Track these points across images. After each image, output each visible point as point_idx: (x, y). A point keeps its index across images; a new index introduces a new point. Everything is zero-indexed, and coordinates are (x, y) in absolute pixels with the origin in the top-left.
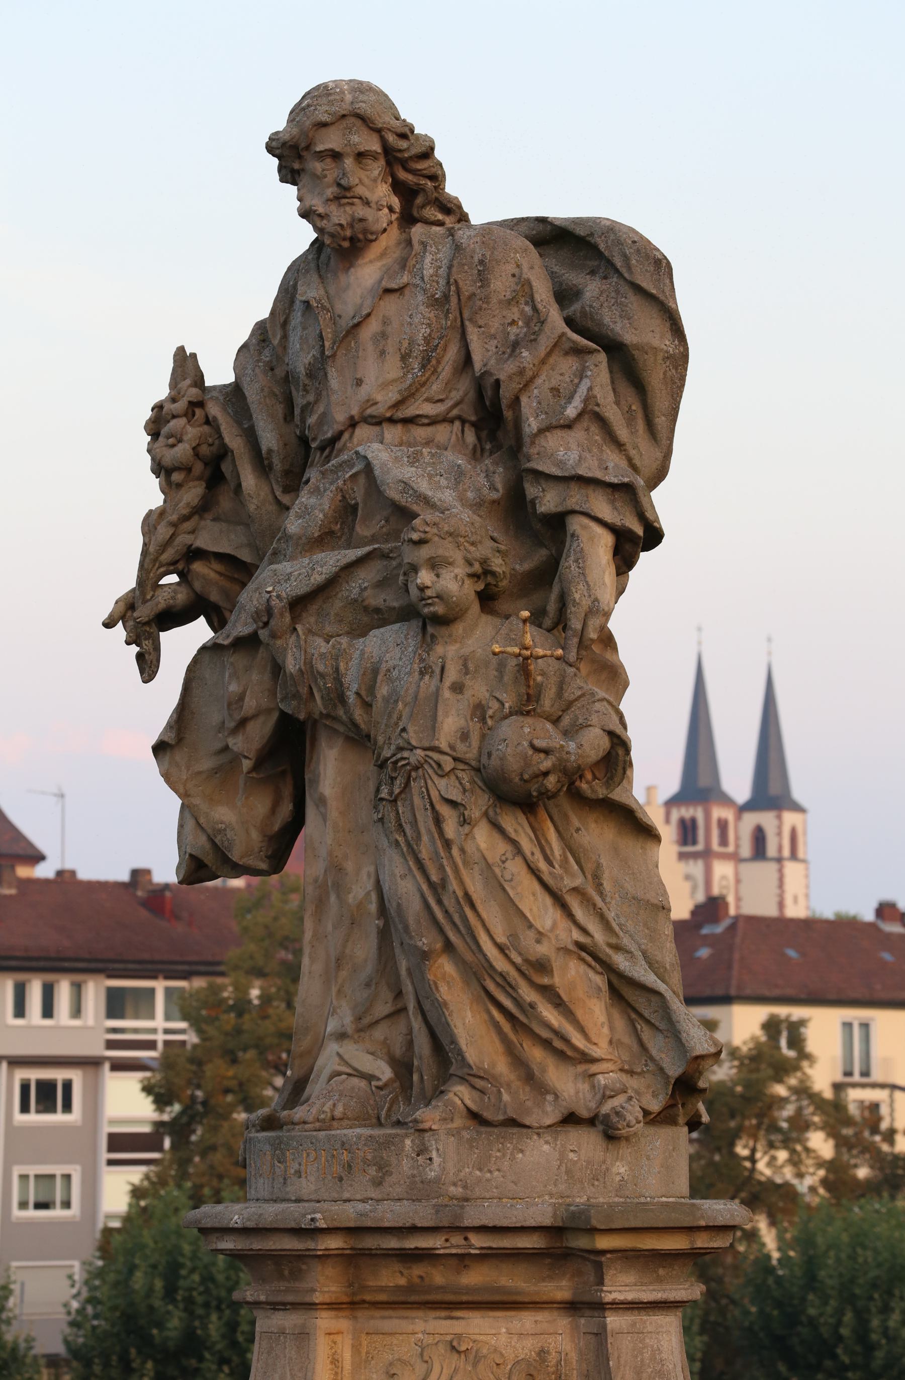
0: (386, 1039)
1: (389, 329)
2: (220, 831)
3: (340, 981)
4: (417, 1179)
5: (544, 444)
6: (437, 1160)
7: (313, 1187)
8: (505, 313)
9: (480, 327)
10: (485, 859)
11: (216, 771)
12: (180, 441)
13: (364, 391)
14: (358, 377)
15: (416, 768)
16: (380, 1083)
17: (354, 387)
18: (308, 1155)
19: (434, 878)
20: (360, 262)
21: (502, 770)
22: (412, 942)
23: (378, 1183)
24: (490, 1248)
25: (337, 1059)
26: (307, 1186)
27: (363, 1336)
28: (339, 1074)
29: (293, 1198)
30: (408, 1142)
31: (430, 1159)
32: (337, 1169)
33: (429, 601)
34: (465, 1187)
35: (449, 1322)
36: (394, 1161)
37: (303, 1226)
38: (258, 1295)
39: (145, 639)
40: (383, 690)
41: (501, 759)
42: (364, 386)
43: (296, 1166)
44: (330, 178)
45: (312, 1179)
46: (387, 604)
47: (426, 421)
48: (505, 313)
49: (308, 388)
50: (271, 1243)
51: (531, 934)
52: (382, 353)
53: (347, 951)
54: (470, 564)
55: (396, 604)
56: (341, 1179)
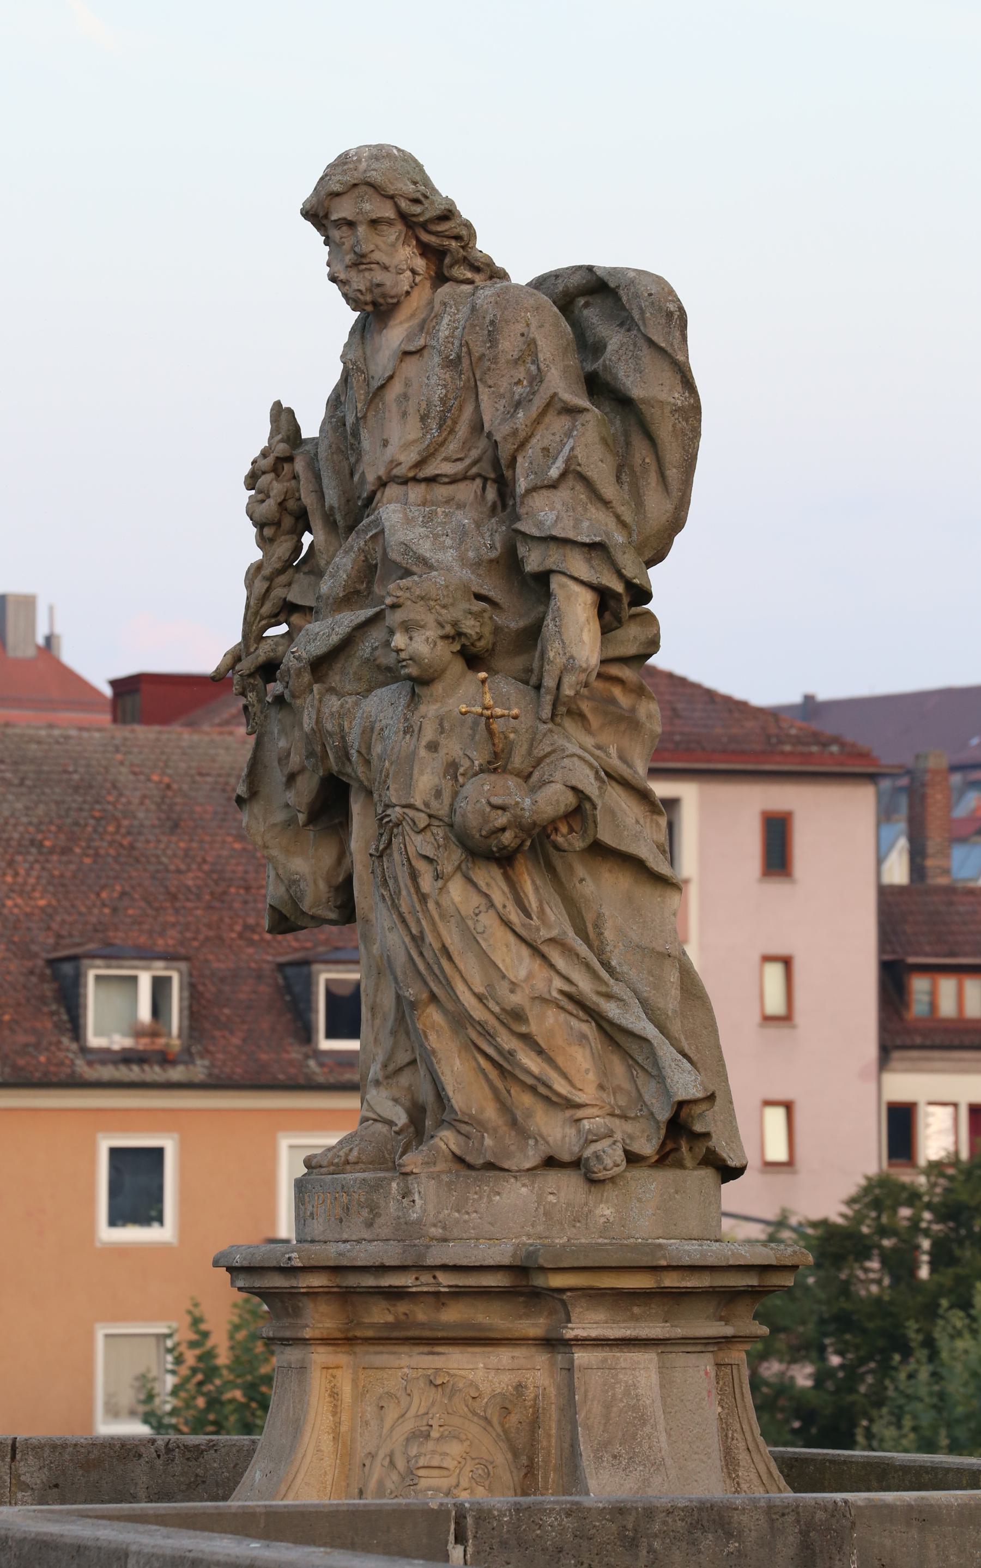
0: (411, 1085)
4: (402, 1220)
5: (531, 504)
8: (512, 373)
9: (490, 387)
10: (459, 912)
12: (268, 497)
13: (391, 450)
14: (385, 437)
15: (397, 825)
19: (414, 931)
20: (392, 323)
21: (464, 826)
23: (369, 1225)
24: (457, 1286)
30: (394, 1185)
31: (414, 1201)
32: (339, 1211)
33: (404, 663)
34: (444, 1228)
35: (430, 1357)
36: (382, 1204)
39: (250, 692)
40: (377, 749)
42: (389, 447)
44: (347, 246)
45: (321, 1220)
47: (446, 480)
48: (512, 373)
50: (266, 1282)
51: (505, 984)
52: (404, 414)
53: (378, 1000)
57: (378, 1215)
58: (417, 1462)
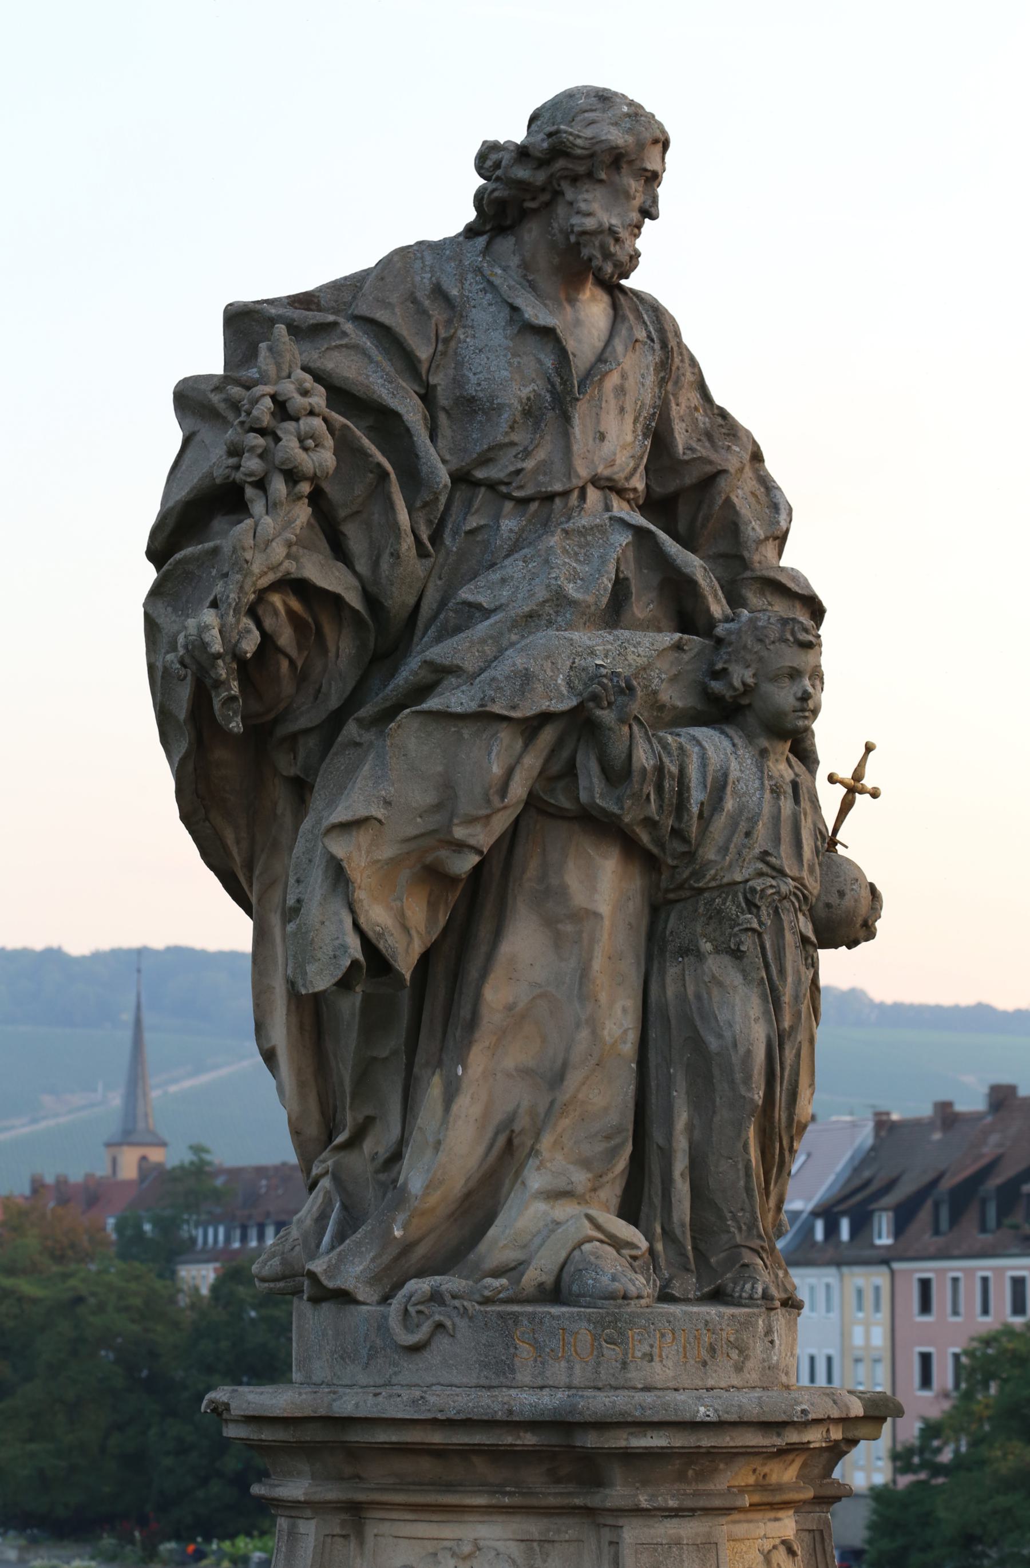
1: (627, 385)
3: (559, 1129)
5: (764, 553)
7: (670, 1373)
13: (607, 447)
16: (634, 1252)
17: (597, 441)
18: (663, 1335)
19: (786, 1024)
22: (750, 1095)
23: (739, 1369)
26: (662, 1372)
28: (590, 1240)
29: (640, 1386)
30: (760, 1322)
36: (752, 1344)
37: (796, 1419)
38: (666, 1501)
41: (856, 901)
42: (606, 442)
43: (646, 1348)
45: (670, 1364)
49: (516, 426)
50: (728, 1439)
55: (679, 704)
56: (705, 1364)
57: (747, 1358)
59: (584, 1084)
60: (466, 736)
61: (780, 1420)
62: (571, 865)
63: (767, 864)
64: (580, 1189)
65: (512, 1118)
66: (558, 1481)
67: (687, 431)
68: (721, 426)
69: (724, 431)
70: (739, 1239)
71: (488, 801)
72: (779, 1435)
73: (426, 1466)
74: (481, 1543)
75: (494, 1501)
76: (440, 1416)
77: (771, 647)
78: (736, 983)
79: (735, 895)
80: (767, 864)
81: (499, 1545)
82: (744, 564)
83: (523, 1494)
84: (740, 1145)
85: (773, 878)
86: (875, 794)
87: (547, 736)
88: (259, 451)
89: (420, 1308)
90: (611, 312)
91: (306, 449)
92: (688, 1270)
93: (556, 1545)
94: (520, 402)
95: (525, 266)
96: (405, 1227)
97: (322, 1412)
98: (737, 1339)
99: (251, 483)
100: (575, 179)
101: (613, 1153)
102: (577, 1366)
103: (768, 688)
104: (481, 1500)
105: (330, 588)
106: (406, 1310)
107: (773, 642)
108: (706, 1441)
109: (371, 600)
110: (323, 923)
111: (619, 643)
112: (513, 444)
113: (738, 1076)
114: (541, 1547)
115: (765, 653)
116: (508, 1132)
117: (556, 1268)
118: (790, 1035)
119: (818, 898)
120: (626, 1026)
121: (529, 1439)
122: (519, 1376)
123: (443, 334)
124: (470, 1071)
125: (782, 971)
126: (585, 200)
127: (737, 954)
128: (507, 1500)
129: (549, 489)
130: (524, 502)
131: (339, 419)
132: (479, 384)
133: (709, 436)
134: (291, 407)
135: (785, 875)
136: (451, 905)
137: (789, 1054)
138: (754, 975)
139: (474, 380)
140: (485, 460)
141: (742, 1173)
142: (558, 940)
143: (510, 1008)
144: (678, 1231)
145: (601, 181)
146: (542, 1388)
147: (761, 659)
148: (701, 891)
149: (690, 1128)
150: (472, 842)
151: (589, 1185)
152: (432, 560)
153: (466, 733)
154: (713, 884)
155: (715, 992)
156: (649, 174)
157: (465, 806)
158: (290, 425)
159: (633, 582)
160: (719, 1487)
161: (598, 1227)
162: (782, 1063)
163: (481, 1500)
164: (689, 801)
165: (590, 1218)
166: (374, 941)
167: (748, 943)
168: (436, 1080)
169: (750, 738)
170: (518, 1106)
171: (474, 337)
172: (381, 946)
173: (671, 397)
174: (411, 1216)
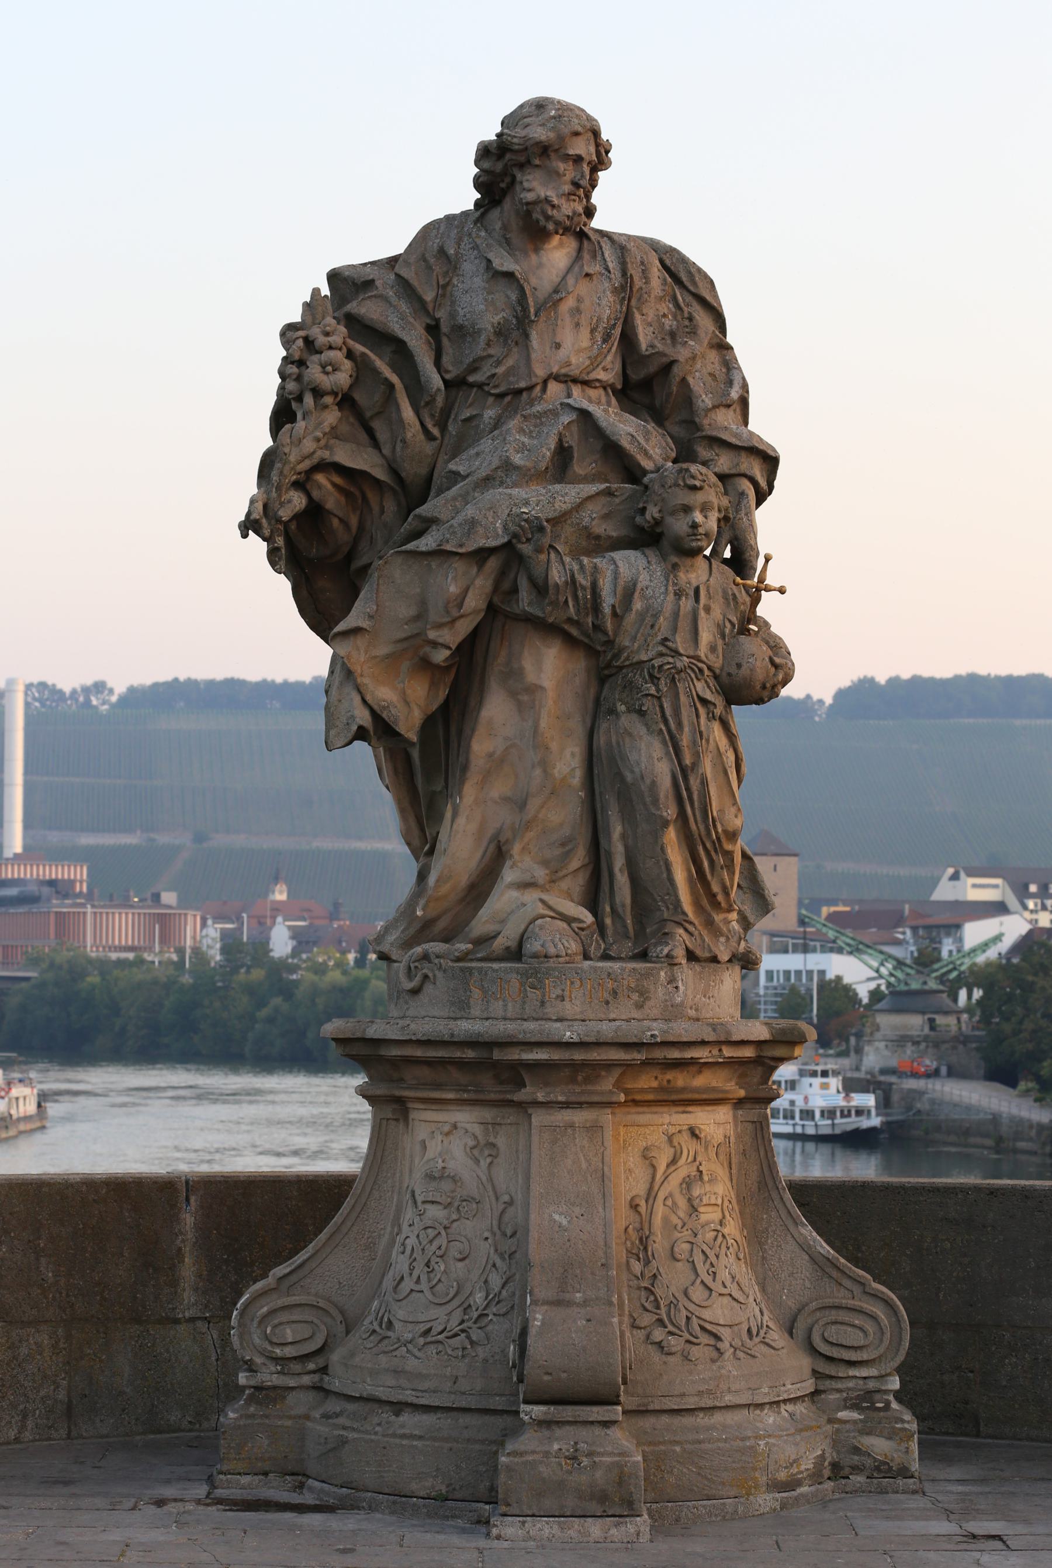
0: (569, 889)
1: (582, 306)
2: (384, 707)
3: (526, 840)
5: (714, 417)
6: (682, 988)
7: (578, 1009)
8: (657, 306)
10: (718, 749)
11: (388, 656)
13: (562, 353)
14: (557, 341)
15: (680, 672)
17: (553, 349)
18: (572, 983)
19: (688, 761)
20: (546, 246)
21: (751, 678)
22: (659, 813)
23: (639, 1006)
24: (732, 1057)
25: (540, 904)
26: (570, 1009)
27: (621, 1128)
28: (543, 917)
29: (554, 1018)
30: (662, 974)
31: (677, 988)
33: (699, 537)
34: (697, 1010)
35: (684, 1116)
36: (652, 987)
37: (645, 1041)
38: (557, 1096)
40: (638, 605)
41: (751, 670)
44: (569, 177)
45: (578, 1003)
46: (607, 533)
48: (658, 306)
49: (491, 343)
51: (733, 810)
53: (540, 816)
54: (719, 511)
55: (614, 534)
56: (607, 1003)
57: (648, 998)
58: (701, 1200)
59: (542, 807)
60: (434, 567)
61: (631, 1041)
62: (526, 653)
63: (667, 647)
64: (541, 881)
65: (499, 831)
66: (502, 1083)
67: (654, 333)
68: (687, 326)
69: (687, 330)
70: (666, 915)
71: (448, 612)
72: (639, 1052)
73: (425, 1072)
74: (459, 1125)
75: (458, 1096)
76: (414, 1038)
77: (669, 491)
78: (641, 734)
79: (643, 671)
80: (667, 647)
81: (468, 1126)
82: (698, 428)
83: (475, 1091)
84: (658, 849)
85: (673, 657)
86: (782, 591)
87: (493, 564)
88: (294, 377)
89: (416, 964)
90: (574, 254)
91: (327, 373)
92: (628, 938)
93: (503, 1127)
94: (493, 326)
95: (505, 228)
96: (423, 909)
97: (358, 1035)
98: (637, 986)
99: (293, 399)
100: (521, 166)
101: (567, 856)
102: (510, 1004)
103: (669, 520)
104: (451, 1096)
105: (357, 467)
106: (410, 968)
107: (670, 487)
108: (578, 1056)
109: (394, 472)
110: (340, 701)
111: (550, 494)
112: (490, 356)
113: (648, 800)
114: (493, 1128)
115: (665, 495)
116: (496, 842)
117: (517, 937)
118: (693, 770)
119: (722, 669)
120: (573, 766)
121: (470, 1054)
122: (472, 1011)
123: (441, 282)
124: (465, 800)
125: (680, 725)
126: (527, 180)
127: (642, 713)
128: (465, 1096)
129: (516, 386)
130: (501, 396)
131: (359, 348)
132: (465, 316)
133: (673, 335)
134: (317, 344)
135: (681, 655)
136: (449, 684)
137: (694, 783)
138: (654, 727)
139: (461, 312)
140: (473, 368)
141: (663, 868)
142: (520, 707)
143: (490, 755)
144: (620, 910)
145: (537, 166)
146: (487, 1019)
147: (663, 500)
148: (621, 668)
149: (624, 837)
150: (441, 640)
151: (547, 878)
152: (438, 441)
153: (434, 565)
154: (627, 663)
155: (627, 740)
156: (575, 157)
157: (433, 616)
158: (315, 358)
159: (575, 449)
160: (603, 1088)
161: (550, 908)
162: (688, 789)
163: (451, 1096)
164: (601, 605)
165: (542, 901)
166: (379, 712)
167: (648, 704)
168: (449, 805)
169: (664, 557)
170: (503, 824)
171: (463, 282)
172: (384, 715)
173: (635, 310)
174: (428, 902)
